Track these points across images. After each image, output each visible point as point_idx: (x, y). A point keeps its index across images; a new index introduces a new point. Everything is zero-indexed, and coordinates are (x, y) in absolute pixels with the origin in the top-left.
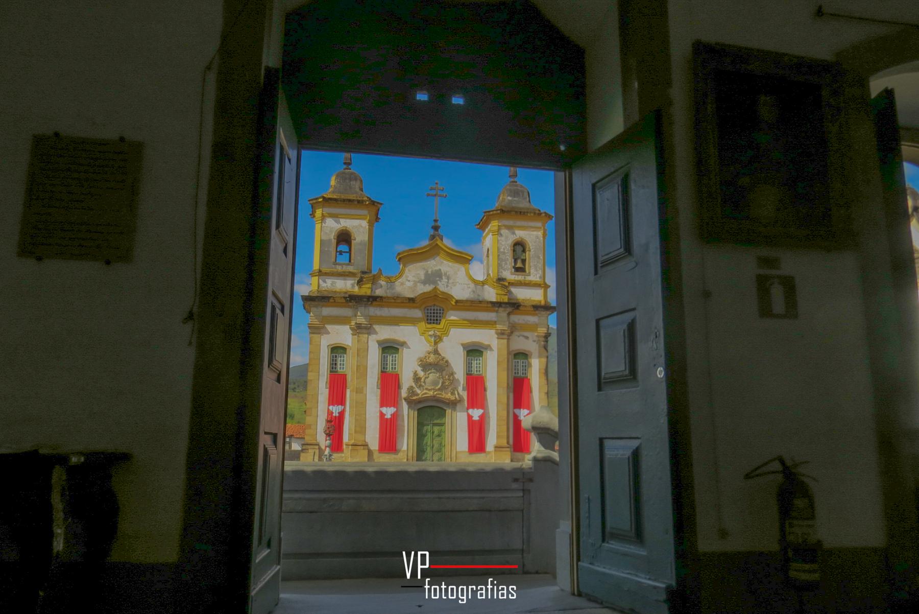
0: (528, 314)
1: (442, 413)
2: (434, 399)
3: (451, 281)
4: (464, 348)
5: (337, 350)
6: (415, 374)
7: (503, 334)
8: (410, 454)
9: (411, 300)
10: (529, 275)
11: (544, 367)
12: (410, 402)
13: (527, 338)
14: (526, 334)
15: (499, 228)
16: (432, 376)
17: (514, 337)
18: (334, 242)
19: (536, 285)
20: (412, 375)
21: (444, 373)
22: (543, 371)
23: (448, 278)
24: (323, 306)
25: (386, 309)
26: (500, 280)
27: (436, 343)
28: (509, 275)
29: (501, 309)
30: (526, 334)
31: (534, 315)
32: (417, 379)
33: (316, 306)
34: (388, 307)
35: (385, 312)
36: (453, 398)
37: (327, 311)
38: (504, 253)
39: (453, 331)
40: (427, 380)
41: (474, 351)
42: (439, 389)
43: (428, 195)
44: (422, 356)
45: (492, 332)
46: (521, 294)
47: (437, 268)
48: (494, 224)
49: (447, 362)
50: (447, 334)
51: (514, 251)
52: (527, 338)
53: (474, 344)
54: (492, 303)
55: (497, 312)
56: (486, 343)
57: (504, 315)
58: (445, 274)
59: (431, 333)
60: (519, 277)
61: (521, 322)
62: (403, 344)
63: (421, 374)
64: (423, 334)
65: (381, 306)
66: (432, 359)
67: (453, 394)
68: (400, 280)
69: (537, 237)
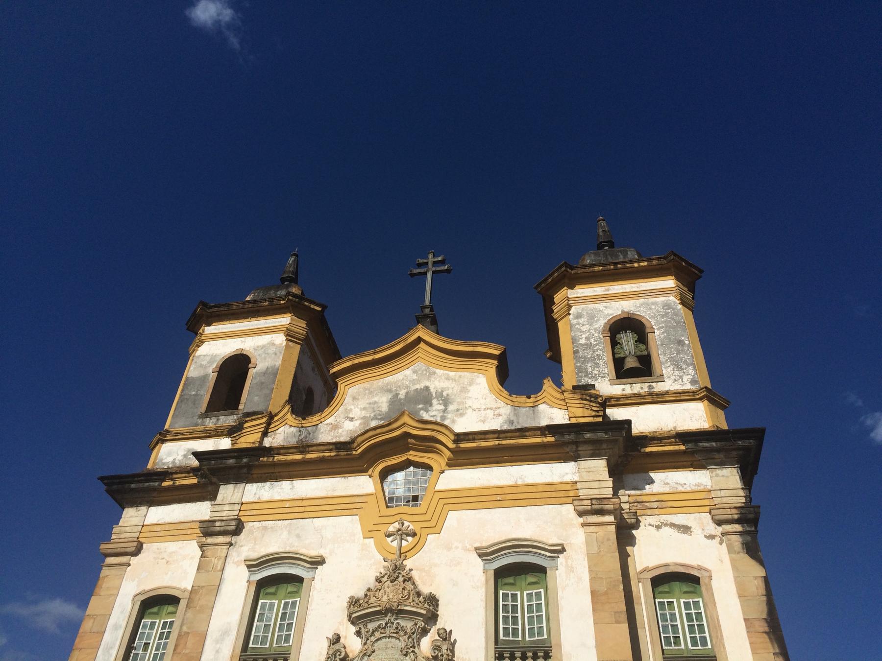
3: (451, 408)
5: (155, 603)
6: (337, 639)
7: (601, 512)
10: (661, 379)
13: (685, 529)
14: (680, 519)
18: (213, 377)
19: (680, 397)
22: (763, 627)
23: (446, 402)
25: (286, 484)
26: (584, 391)
27: (403, 554)
28: (606, 387)
30: (680, 519)
33: (135, 503)
38: (589, 346)
39: (454, 518)
41: (517, 570)
44: (359, 592)
45: (568, 510)
46: (645, 420)
47: (418, 386)
49: (433, 600)
50: (436, 527)
51: (614, 343)
52: (685, 529)
53: (518, 546)
54: (552, 429)
58: (440, 395)
59: (391, 529)
60: (638, 387)
62: (317, 562)
63: (353, 644)
64: (369, 533)
68: (330, 420)
69: (667, 306)
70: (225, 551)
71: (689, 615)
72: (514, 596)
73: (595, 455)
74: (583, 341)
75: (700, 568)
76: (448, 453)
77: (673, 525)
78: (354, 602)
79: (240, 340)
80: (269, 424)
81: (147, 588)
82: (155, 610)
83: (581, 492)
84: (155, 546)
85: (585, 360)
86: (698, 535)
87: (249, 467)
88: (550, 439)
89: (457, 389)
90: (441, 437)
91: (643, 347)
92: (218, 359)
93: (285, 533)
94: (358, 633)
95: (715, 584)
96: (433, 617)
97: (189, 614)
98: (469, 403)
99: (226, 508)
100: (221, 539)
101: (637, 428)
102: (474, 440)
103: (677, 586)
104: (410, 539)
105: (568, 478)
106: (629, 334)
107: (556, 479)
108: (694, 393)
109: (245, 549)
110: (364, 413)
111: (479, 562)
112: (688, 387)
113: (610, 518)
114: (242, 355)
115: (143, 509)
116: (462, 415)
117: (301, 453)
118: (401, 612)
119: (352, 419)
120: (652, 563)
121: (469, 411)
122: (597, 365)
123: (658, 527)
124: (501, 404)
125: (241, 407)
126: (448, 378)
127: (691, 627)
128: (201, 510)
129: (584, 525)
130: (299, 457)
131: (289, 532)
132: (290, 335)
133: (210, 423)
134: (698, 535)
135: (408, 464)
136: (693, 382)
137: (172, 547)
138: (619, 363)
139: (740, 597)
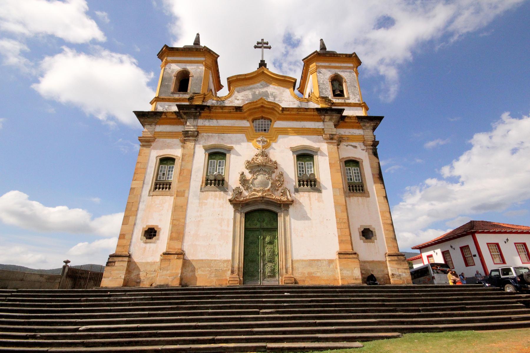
0: (353, 127)
1: (275, 216)
2: (263, 200)
3: (277, 99)
4: (293, 152)
6: (243, 173)
7: (332, 139)
8: (236, 265)
9: (238, 109)
10: (348, 98)
11: (377, 172)
12: (236, 204)
13: (355, 147)
14: (354, 144)
15: (318, 67)
16: (261, 178)
17: (343, 145)
18: (174, 79)
20: (238, 176)
21: (274, 176)
22: (377, 176)
23: (275, 97)
24: (156, 124)
25: (215, 121)
29: (327, 118)
30: (354, 144)
31: (358, 128)
32: (244, 181)
33: (150, 124)
34: (217, 118)
35: (214, 123)
36: (284, 199)
37: (159, 128)
38: (324, 84)
40: (256, 182)
41: (304, 156)
42: (269, 190)
43: (256, 47)
48: (313, 66)
51: (332, 85)
52: (355, 147)
53: (305, 148)
54: (318, 110)
55: (323, 122)
56: (316, 147)
57: (331, 124)
58: (272, 94)
61: (347, 134)
63: (249, 176)
65: (210, 118)
66: (260, 159)
67: (284, 194)
68: (230, 99)
70: (193, 143)
71: (355, 173)
72: (302, 164)
73: (330, 120)
74: (321, 82)
75: (359, 159)
76: (278, 115)
77: (351, 145)
78: (248, 162)
79: (184, 64)
80: (204, 98)
81: (161, 154)
82: (165, 162)
83: (325, 132)
84: (161, 140)
85: (322, 89)
86: (359, 149)
87: (200, 113)
88: (316, 113)
89: (278, 93)
90: (276, 109)
91: (341, 87)
92: (175, 71)
93: (217, 138)
94: (250, 172)
95: (364, 163)
96: (277, 168)
97: (183, 163)
98: (283, 98)
99: (192, 127)
100: (191, 138)
101: (345, 114)
102: (288, 111)
103: (351, 163)
104: (266, 143)
105: (321, 127)
106: (337, 82)
107: (316, 127)
108: (360, 104)
109: (201, 142)
110: (242, 98)
111: (291, 153)
112: (357, 102)
113: (335, 141)
114: (186, 71)
115: (154, 126)
116: (281, 102)
117: (222, 109)
118: (265, 166)
119: (238, 100)
120: (345, 157)
121: (284, 102)
122: (326, 91)
123: (347, 146)
124: (295, 100)
125: (188, 91)
126: (274, 89)
127: (355, 176)
128: (179, 128)
129: (327, 143)
130: (221, 110)
131: (219, 138)
132: (206, 66)
133: (176, 96)
134: (359, 149)
135: (262, 118)
136: (359, 101)
137: (168, 140)
138: (334, 91)
139: (372, 167)
